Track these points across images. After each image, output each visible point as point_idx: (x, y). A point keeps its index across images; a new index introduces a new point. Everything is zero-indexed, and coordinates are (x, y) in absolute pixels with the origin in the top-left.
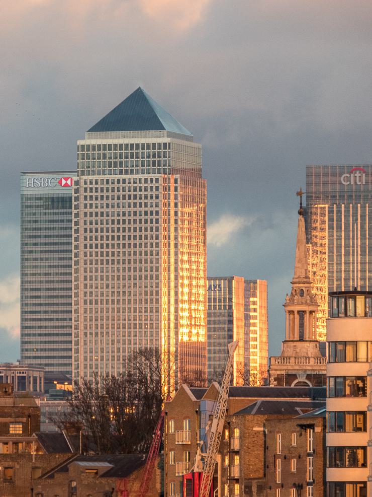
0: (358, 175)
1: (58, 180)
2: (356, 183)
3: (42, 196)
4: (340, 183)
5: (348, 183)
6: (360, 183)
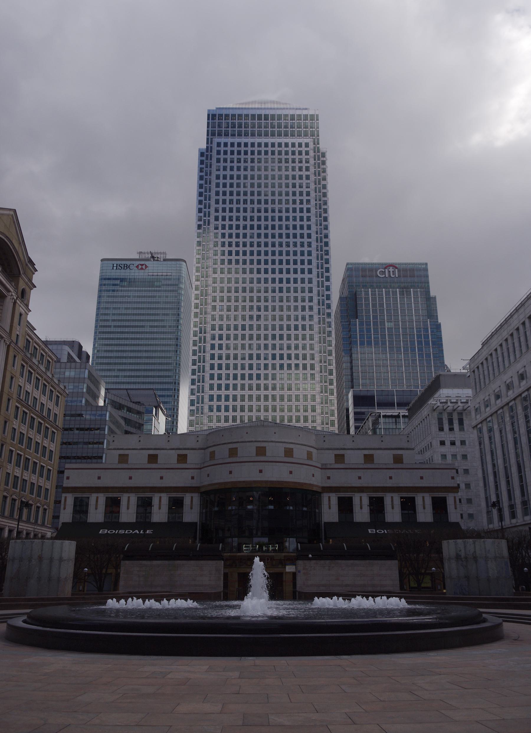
0: (391, 269)
1: (136, 265)
2: (390, 276)
3: (119, 277)
4: (377, 276)
5: (384, 276)
6: (393, 276)
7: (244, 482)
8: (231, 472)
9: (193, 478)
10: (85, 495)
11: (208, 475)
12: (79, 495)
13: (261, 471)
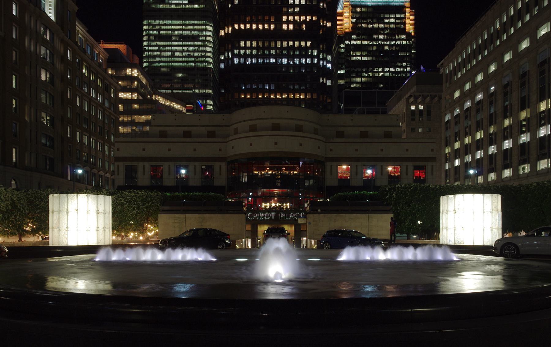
7: (262, 152)
8: (251, 145)
9: (220, 150)
10: (134, 163)
11: (233, 148)
12: (129, 163)
13: (276, 144)
